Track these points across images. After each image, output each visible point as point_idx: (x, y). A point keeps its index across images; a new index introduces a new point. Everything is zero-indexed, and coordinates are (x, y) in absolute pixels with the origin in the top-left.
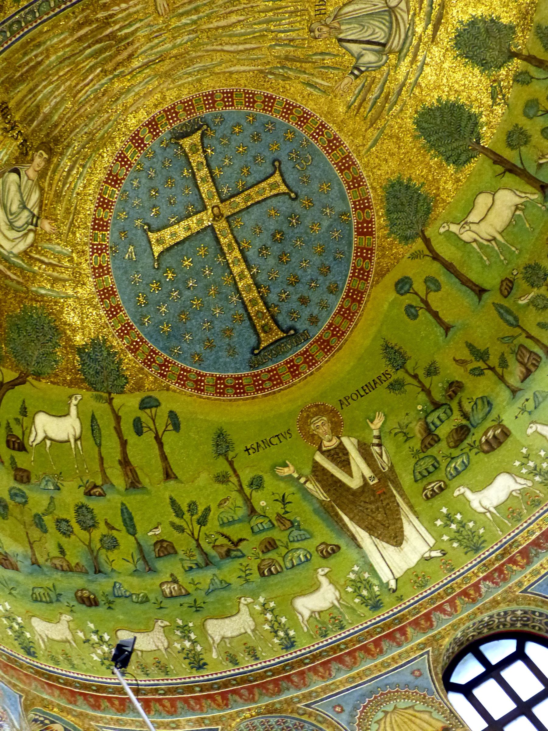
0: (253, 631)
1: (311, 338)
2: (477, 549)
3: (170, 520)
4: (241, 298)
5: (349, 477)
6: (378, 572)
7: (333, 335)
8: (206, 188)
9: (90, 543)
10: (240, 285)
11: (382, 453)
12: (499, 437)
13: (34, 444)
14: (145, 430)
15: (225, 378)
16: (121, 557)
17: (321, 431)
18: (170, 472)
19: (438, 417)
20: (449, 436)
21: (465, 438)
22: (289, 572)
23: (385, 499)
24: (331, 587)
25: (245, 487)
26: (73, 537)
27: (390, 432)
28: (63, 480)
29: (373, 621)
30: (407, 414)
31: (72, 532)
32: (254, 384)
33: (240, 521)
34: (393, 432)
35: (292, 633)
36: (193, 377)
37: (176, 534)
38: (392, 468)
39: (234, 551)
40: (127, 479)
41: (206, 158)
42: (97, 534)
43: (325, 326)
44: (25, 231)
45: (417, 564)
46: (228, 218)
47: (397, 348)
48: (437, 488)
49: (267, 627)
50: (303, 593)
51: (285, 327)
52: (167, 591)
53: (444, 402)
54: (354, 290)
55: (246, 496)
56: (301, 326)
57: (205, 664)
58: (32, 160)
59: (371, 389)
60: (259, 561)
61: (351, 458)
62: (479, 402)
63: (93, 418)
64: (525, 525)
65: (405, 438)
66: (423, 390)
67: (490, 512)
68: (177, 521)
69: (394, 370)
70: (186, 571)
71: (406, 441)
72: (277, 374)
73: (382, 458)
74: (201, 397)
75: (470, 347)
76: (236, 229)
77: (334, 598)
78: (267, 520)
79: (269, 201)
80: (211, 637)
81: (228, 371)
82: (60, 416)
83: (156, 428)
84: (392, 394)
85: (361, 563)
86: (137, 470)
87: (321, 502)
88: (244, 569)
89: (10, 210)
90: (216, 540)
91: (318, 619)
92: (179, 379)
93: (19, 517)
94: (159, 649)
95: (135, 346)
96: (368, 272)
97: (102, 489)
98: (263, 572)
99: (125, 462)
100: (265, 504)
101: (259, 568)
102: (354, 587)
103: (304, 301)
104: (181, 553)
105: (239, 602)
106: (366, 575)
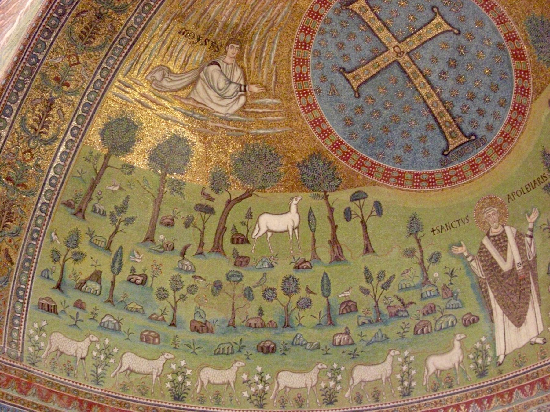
0: (387, 378)
1: (488, 143)
3: (361, 285)
4: (431, 111)
5: (504, 261)
6: (497, 345)
7: (505, 141)
8: (384, 35)
9: (287, 305)
10: (429, 102)
13: (257, 237)
14: (353, 216)
15: (421, 174)
16: (310, 314)
17: (491, 219)
18: (369, 247)
22: (434, 333)
23: (523, 284)
24: (460, 351)
25: (425, 261)
26: (275, 301)
27: (541, 227)
28: (278, 260)
31: (275, 298)
32: (443, 179)
35: (414, 384)
36: (395, 174)
37: (362, 295)
38: (535, 258)
40: (333, 254)
41: (375, 14)
42: (295, 298)
43: (498, 133)
44: (237, 97)
45: (524, 346)
46: (408, 54)
49: (399, 376)
50: (438, 353)
51: (467, 134)
52: (338, 341)
54: (519, 104)
55: (425, 268)
56: (481, 132)
57: (336, 401)
58: (226, 52)
60: (418, 321)
61: (508, 245)
63: (311, 212)
68: (366, 286)
70: (359, 325)
72: (462, 171)
73: (530, 248)
74: (400, 189)
76: (416, 61)
77: (457, 360)
78: (435, 288)
79: (438, 37)
80: (353, 379)
81: (424, 169)
82: (282, 214)
83: (362, 215)
84: (546, 194)
86: (342, 246)
88: (404, 327)
89: (218, 88)
91: (438, 376)
92: (383, 176)
93: (230, 292)
94: (306, 387)
95: (346, 156)
96: (528, 89)
97: (310, 264)
98: (417, 331)
99: (334, 242)
100: (437, 276)
101: (416, 327)
102: (475, 355)
103: (481, 112)
104: (360, 311)
105: (389, 354)
106: (488, 346)
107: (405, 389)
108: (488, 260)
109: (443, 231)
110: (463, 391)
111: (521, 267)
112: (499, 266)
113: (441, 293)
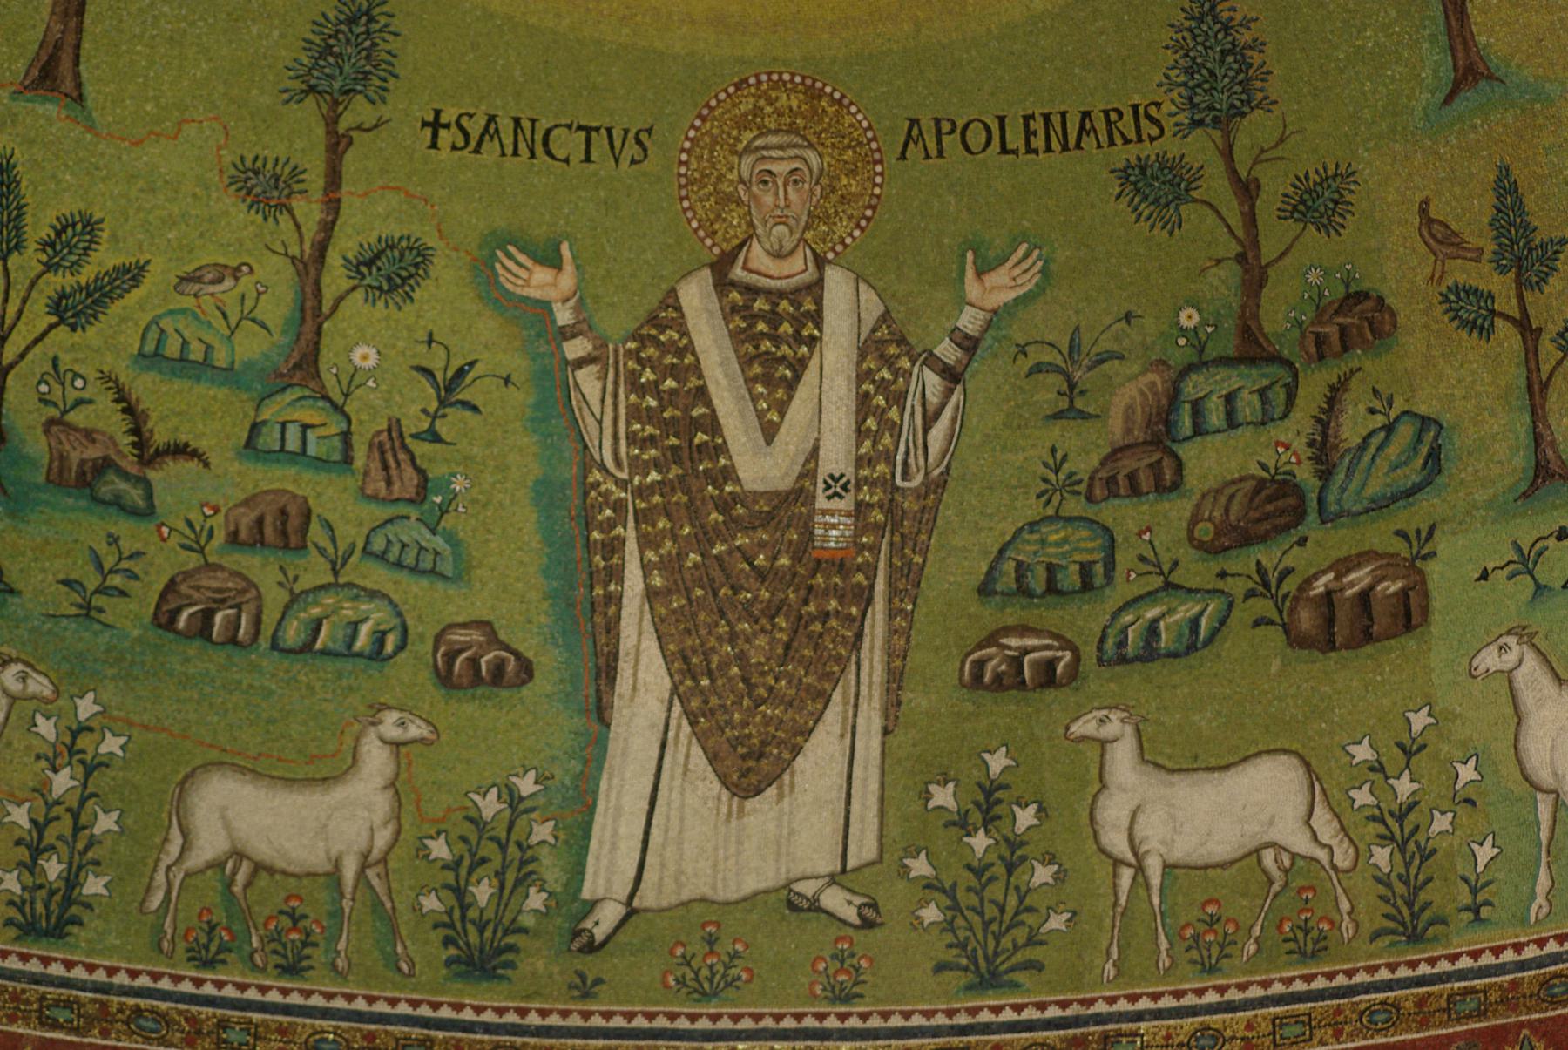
2: (989, 980)
6: (594, 844)
12: (1377, 609)
17: (768, 199)
19: (1229, 399)
20: (1218, 491)
21: (1263, 538)
25: (334, 258)
29: (424, 1011)
30: (1128, 317)
33: (228, 375)
34: (1037, 355)
35: (93, 886)
39: (125, 475)
47: (1245, 37)
48: (1034, 663)
49: (20, 816)
53: (1285, 353)
59: (1055, 145)
60: (193, 560)
61: (814, 364)
62: (1405, 431)
64: (1211, 997)
65: (1063, 404)
66: (1241, 258)
67: (1140, 869)
69: (1183, 118)
71: (1058, 415)
73: (926, 430)
75: (1507, 190)
77: (362, 843)
78: (335, 426)
84: (1123, 204)
85: (563, 774)
87: (588, 464)
90: (79, 402)
91: (237, 888)
98: (178, 610)
100: (371, 362)
101: (171, 586)
102: (460, 848)
107: (43, 893)
108: (672, 392)
109: (490, 148)
110: (359, 1016)
111: (846, 503)
112: (723, 449)
113: (360, 460)
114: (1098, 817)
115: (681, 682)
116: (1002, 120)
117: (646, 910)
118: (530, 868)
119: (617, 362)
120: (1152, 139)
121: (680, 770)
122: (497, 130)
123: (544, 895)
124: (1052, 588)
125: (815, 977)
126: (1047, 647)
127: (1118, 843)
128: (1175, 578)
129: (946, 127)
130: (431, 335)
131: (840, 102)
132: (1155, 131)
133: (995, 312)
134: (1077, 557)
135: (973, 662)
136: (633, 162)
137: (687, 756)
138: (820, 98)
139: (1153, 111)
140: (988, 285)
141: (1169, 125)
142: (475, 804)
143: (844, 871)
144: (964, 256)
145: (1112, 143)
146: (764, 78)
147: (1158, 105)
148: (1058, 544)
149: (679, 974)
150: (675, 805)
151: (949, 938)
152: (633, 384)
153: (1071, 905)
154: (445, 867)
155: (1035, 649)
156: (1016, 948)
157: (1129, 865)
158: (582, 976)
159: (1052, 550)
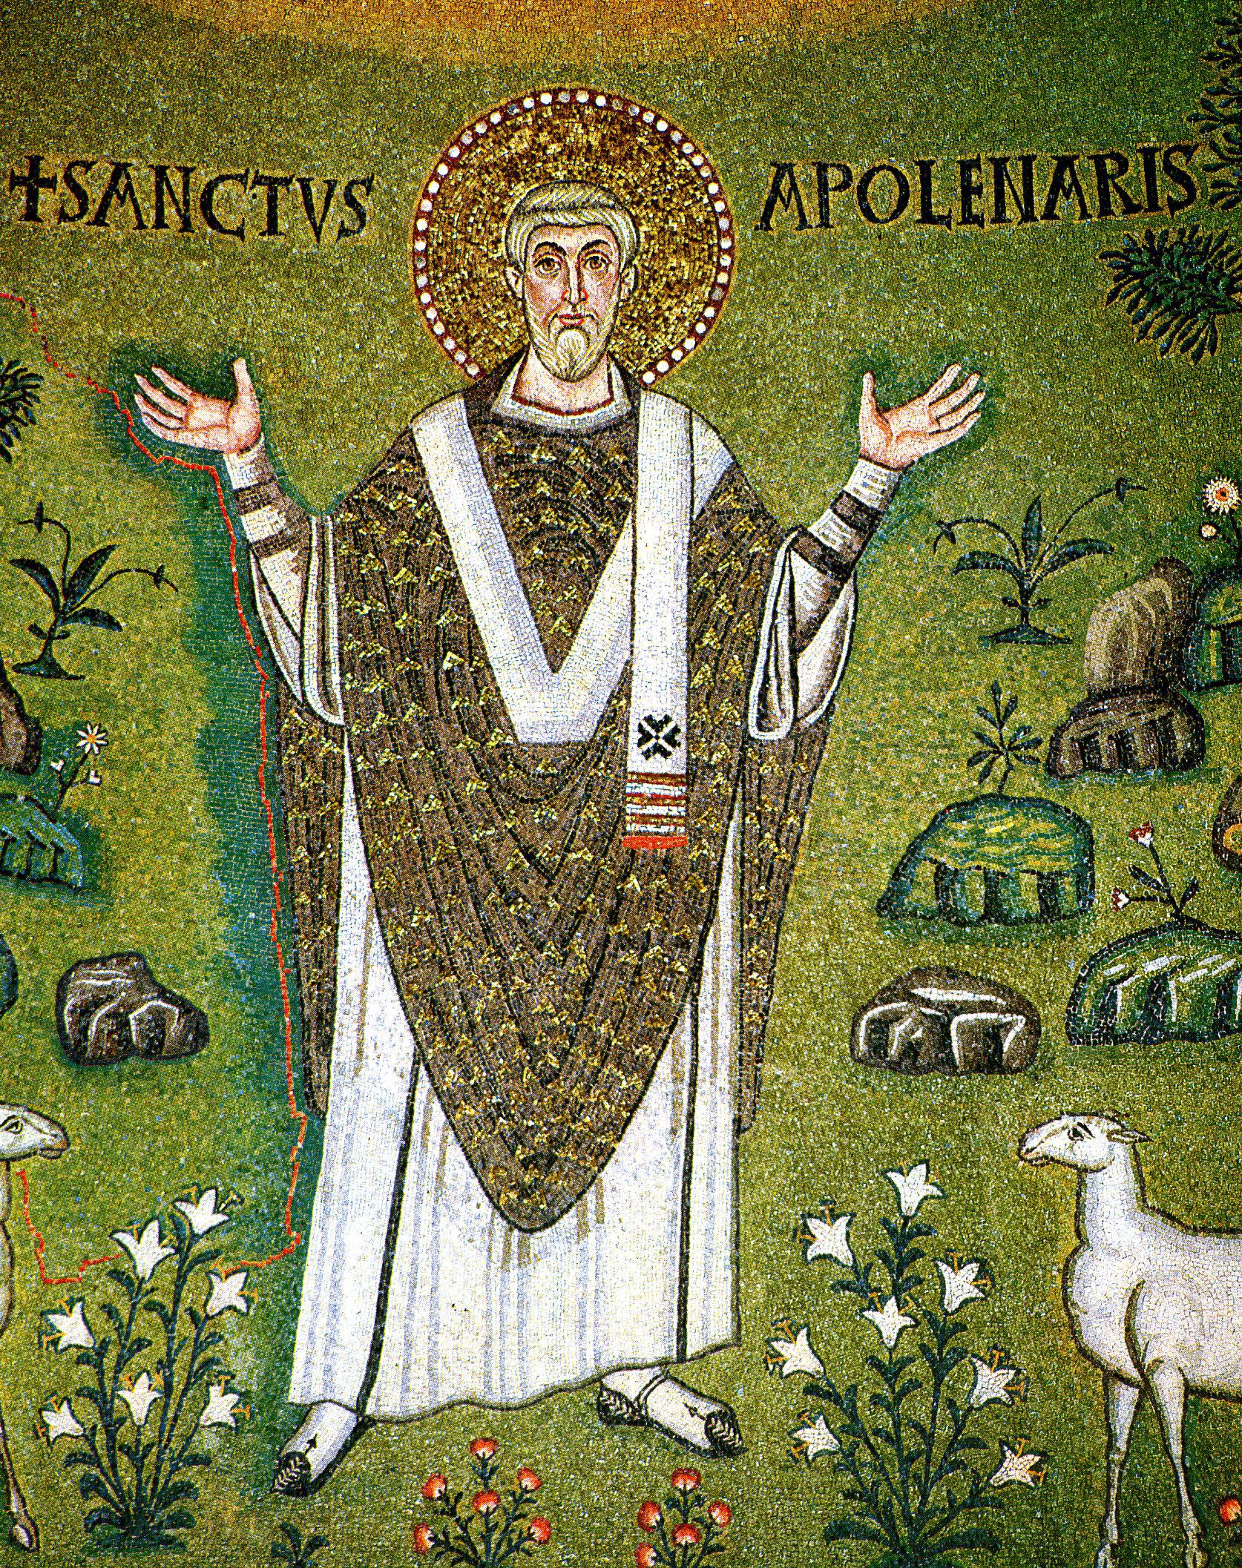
11: (815, 625)
61: (623, 545)
67: (1146, 1391)
73: (795, 652)
111: (675, 763)
114: (1075, 1297)
115: (431, 1043)
116: (925, 167)
117: (387, 1421)
118: (209, 1353)
119: (323, 544)
120: (1174, 205)
121: (429, 1185)
122: (129, 187)
123: (233, 1398)
124: (993, 909)
125: (644, 1538)
126: (986, 1006)
127: (1110, 1345)
128: (1192, 908)
129: (834, 176)
130: (40, 509)
131: (666, 136)
132: (1180, 193)
133: (905, 469)
134: (1033, 863)
135: (872, 1021)
136: (343, 232)
137: (442, 1163)
138: (634, 130)
139: (1179, 161)
140: (895, 427)
141: (1204, 189)
142: (126, 1249)
143: (682, 1357)
144: (858, 381)
145: (1105, 209)
146: (546, 98)
147: (1188, 152)
148: (999, 839)
149: (438, 1528)
150: (425, 1242)
151: (847, 1480)
152: (347, 578)
153: (1040, 1442)
154: (83, 1359)
155: (966, 1007)
156: (954, 1509)
157: (1128, 1382)
158: (291, 1533)
159: (992, 850)
